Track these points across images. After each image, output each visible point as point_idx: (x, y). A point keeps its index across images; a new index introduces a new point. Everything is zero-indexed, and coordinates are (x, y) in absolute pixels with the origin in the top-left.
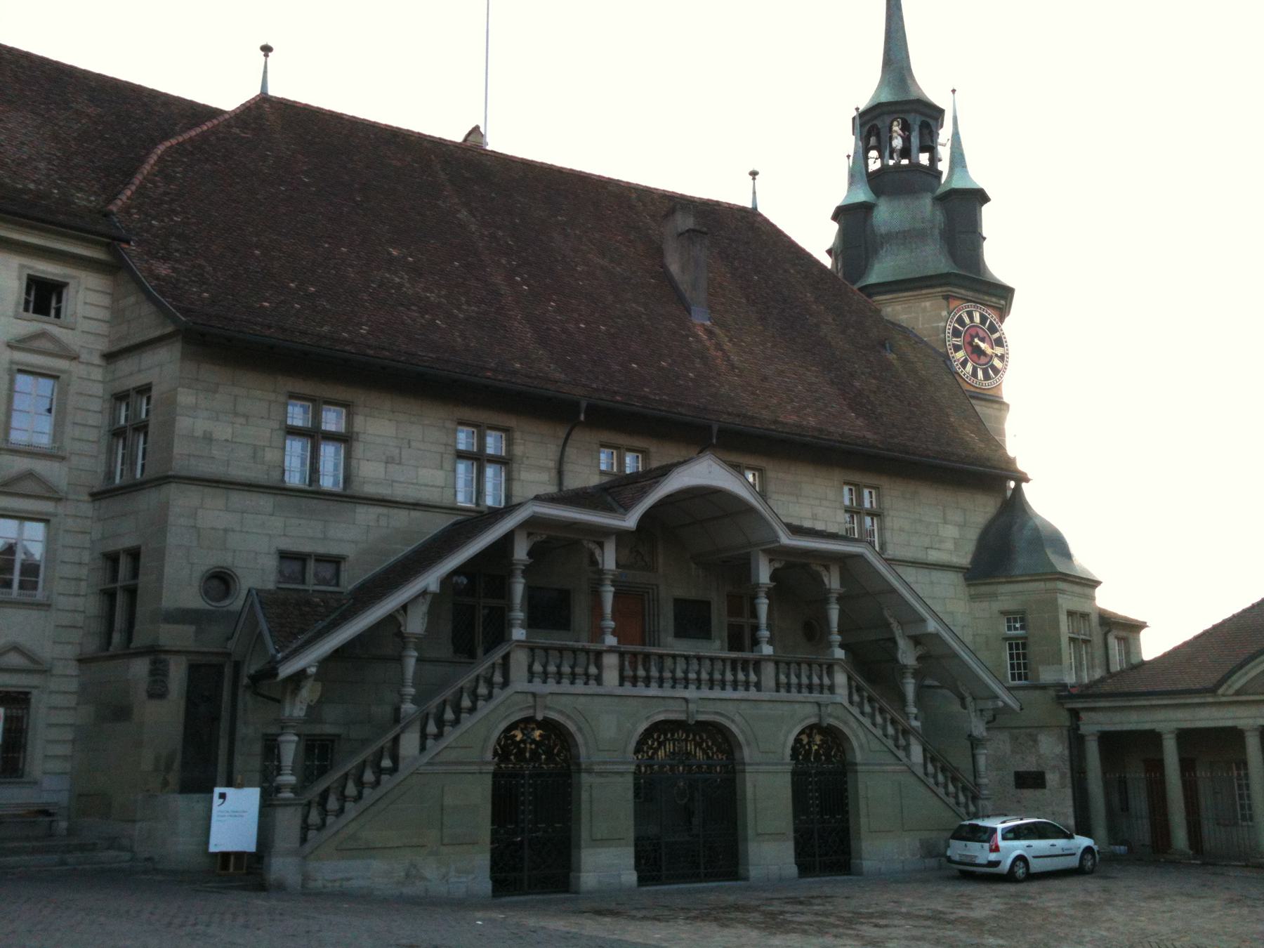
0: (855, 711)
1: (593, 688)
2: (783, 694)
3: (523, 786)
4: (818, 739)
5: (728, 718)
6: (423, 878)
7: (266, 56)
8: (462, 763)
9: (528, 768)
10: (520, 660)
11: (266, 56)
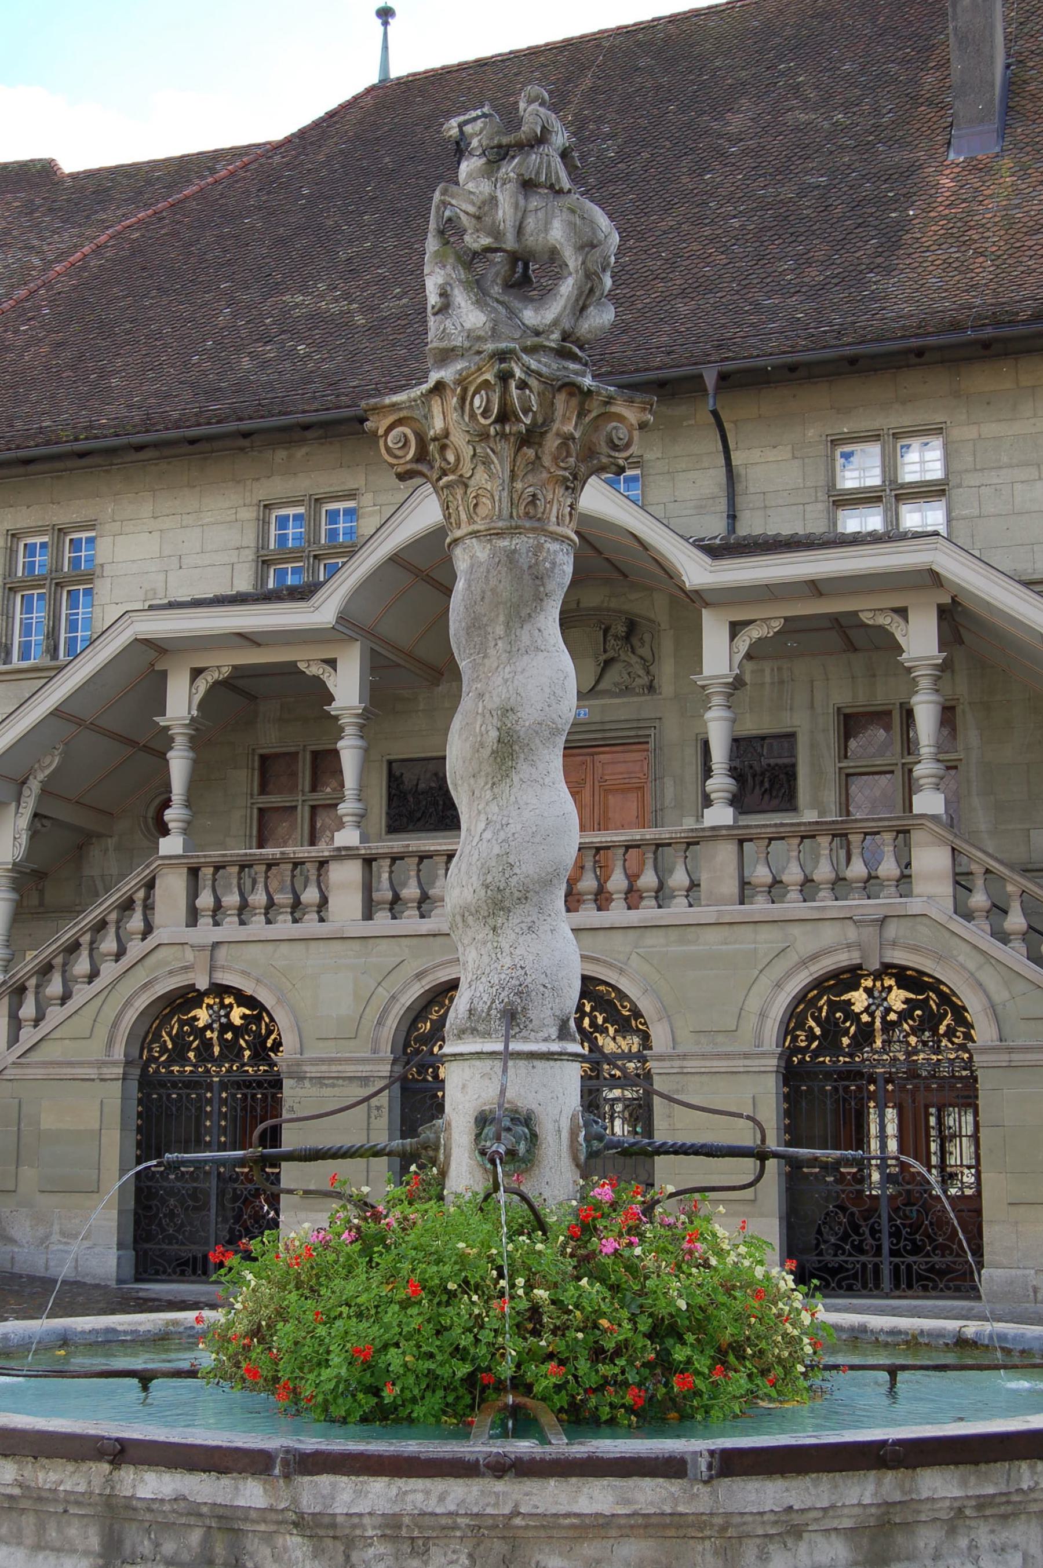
0: (978, 933)
1: (310, 925)
2: (760, 906)
3: (209, 1102)
4: (897, 998)
5: (611, 966)
6: (12, 1241)
7: (386, 24)
8: (71, 1064)
9: (217, 1072)
10: (172, 887)
11: (386, 24)
